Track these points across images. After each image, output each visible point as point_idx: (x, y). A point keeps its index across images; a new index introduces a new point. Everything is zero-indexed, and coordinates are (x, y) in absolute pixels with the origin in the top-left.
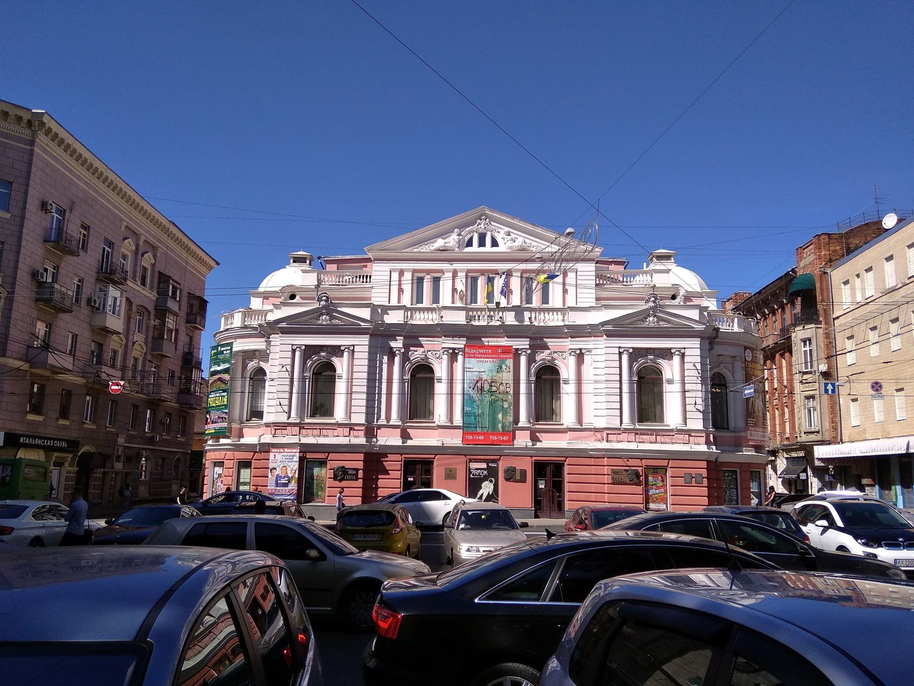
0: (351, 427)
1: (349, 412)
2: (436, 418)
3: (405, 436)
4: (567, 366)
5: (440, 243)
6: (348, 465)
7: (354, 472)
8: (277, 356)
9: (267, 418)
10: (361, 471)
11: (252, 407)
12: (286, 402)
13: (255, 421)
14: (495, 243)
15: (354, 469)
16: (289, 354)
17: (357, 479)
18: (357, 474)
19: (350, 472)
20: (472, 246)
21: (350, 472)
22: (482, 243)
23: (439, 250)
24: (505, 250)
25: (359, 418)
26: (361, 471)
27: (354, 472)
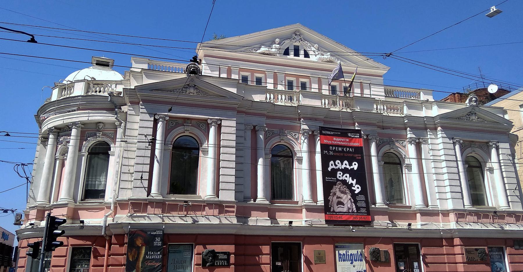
0: (221, 207)
1: (217, 190)
2: (296, 197)
3: (273, 218)
4: (407, 152)
5: (263, 49)
6: (218, 248)
7: (225, 257)
8: (136, 126)
9: (109, 197)
10: (232, 256)
11: (87, 185)
12: (146, 176)
13: (92, 202)
14: (307, 55)
15: (225, 253)
16: (151, 124)
17: (228, 265)
18: (228, 260)
19: (221, 256)
20: (288, 54)
21: (221, 256)
22: (297, 54)
23: (264, 54)
24: (315, 60)
25: (228, 196)
26: (232, 256)
27: (225, 257)
